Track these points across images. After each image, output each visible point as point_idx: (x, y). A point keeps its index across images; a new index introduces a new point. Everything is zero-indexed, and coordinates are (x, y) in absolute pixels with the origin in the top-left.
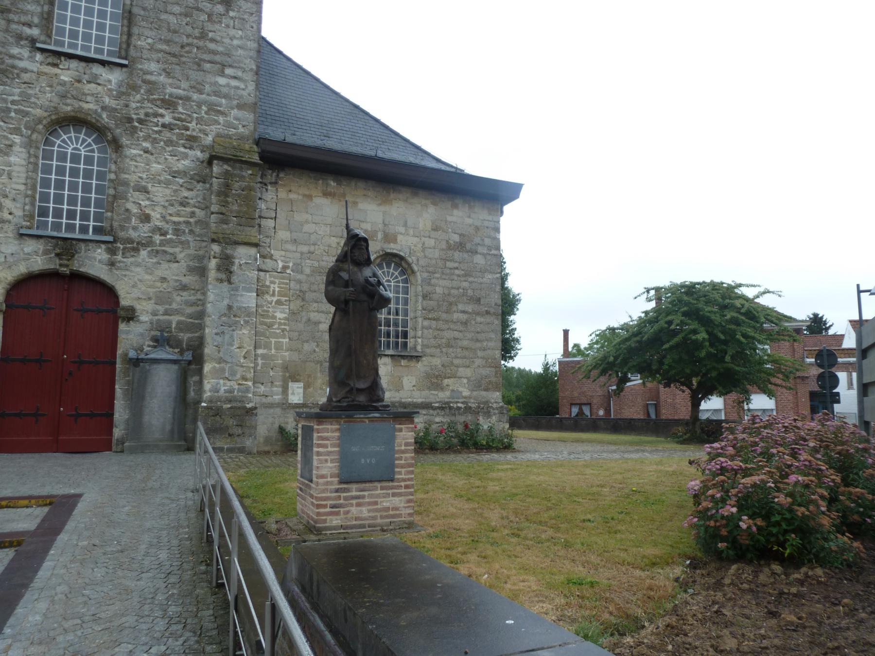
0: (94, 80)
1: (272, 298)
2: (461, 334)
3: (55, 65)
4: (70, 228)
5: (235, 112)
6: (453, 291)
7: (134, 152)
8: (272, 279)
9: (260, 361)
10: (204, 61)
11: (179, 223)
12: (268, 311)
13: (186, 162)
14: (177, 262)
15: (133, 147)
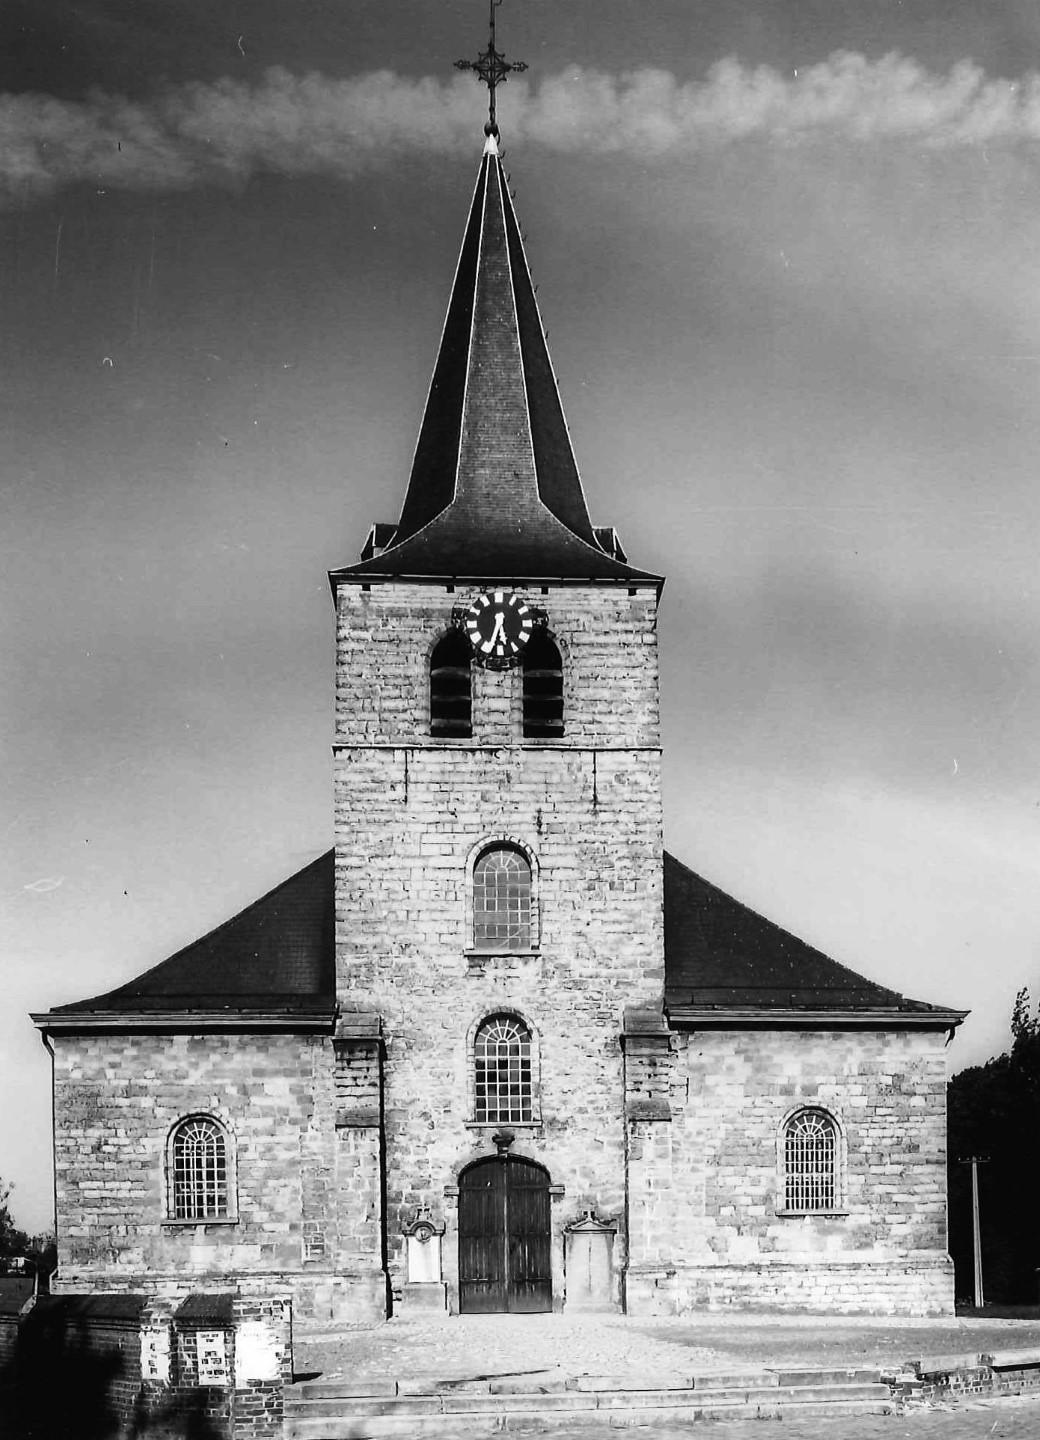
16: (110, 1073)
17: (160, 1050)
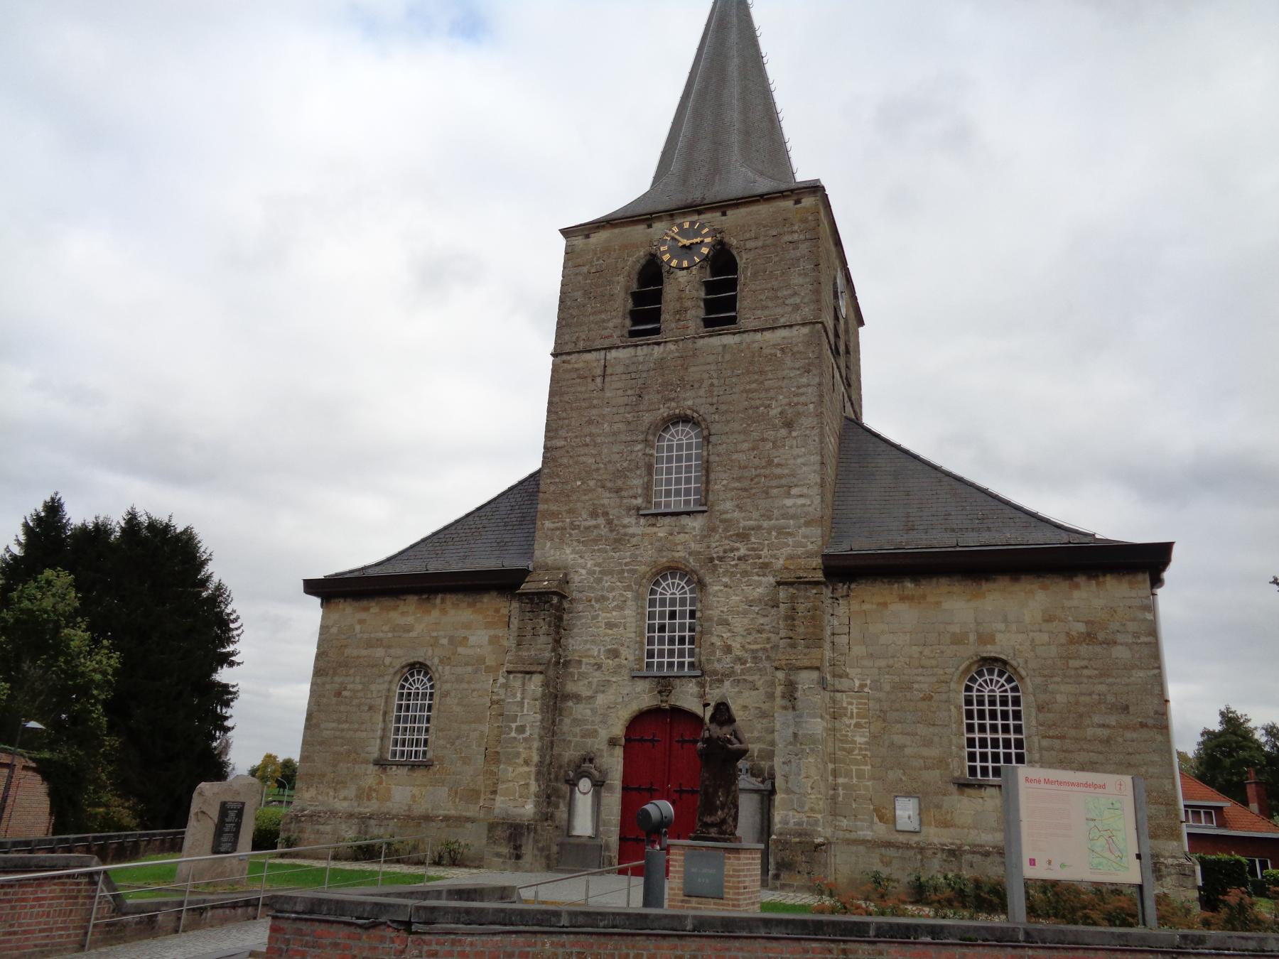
0: (683, 530)
1: (851, 721)
2: (1101, 756)
3: (654, 525)
4: (671, 665)
5: (803, 530)
6: (1082, 699)
7: (716, 588)
8: (849, 700)
9: (841, 791)
10: (772, 487)
11: (757, 650)
12: (847, 736)
13: (760, 590)
14: (757, 689)
15: (715, 584)
16: (358, 628)
17: (396, 608)
